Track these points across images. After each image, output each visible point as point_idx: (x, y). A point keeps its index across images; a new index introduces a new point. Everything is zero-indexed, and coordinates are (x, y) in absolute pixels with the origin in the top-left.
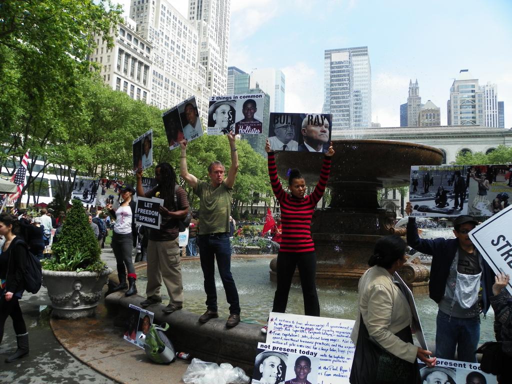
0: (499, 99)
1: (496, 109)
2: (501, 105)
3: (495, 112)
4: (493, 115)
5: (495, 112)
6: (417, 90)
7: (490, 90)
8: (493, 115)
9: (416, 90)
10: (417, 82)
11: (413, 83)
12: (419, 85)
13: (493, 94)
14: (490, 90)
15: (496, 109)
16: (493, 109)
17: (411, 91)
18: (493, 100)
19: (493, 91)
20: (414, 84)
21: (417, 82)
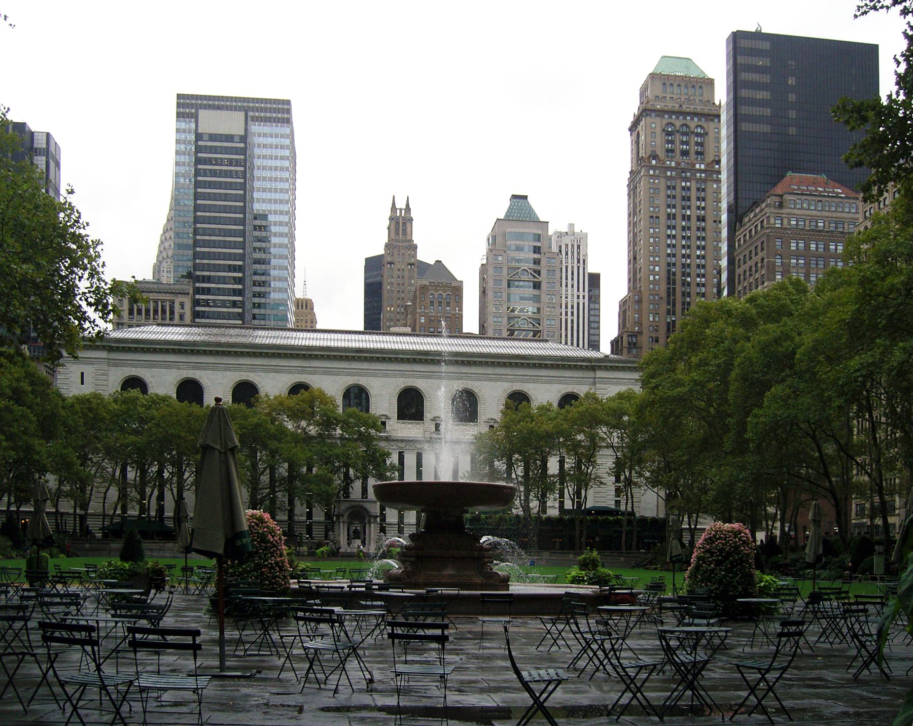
0: (591, 269)
1: (584, 291)
2: (595, 279)
3: (581, 297)
4: (578, 304)
5: (581, 297)
6: (408, 225)
7: (573, 246)
8: (578, 304)
9: (404, 224)
10: (408, 205)
11: (398, 206)
12: (413, 214)
13: (579, 253)
14: (573, 246)
15: (584, 291)
16: (578, 290)
17: (393, 228)
18: (578, 267)
19: (579, 247)
20: (401, 210)
21: (408, 205)
